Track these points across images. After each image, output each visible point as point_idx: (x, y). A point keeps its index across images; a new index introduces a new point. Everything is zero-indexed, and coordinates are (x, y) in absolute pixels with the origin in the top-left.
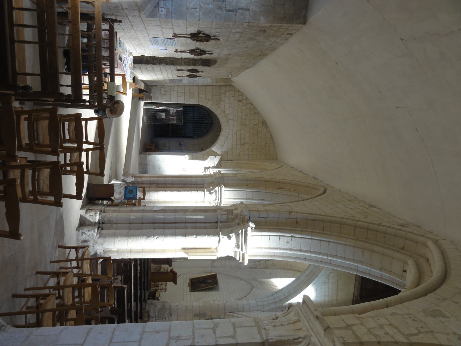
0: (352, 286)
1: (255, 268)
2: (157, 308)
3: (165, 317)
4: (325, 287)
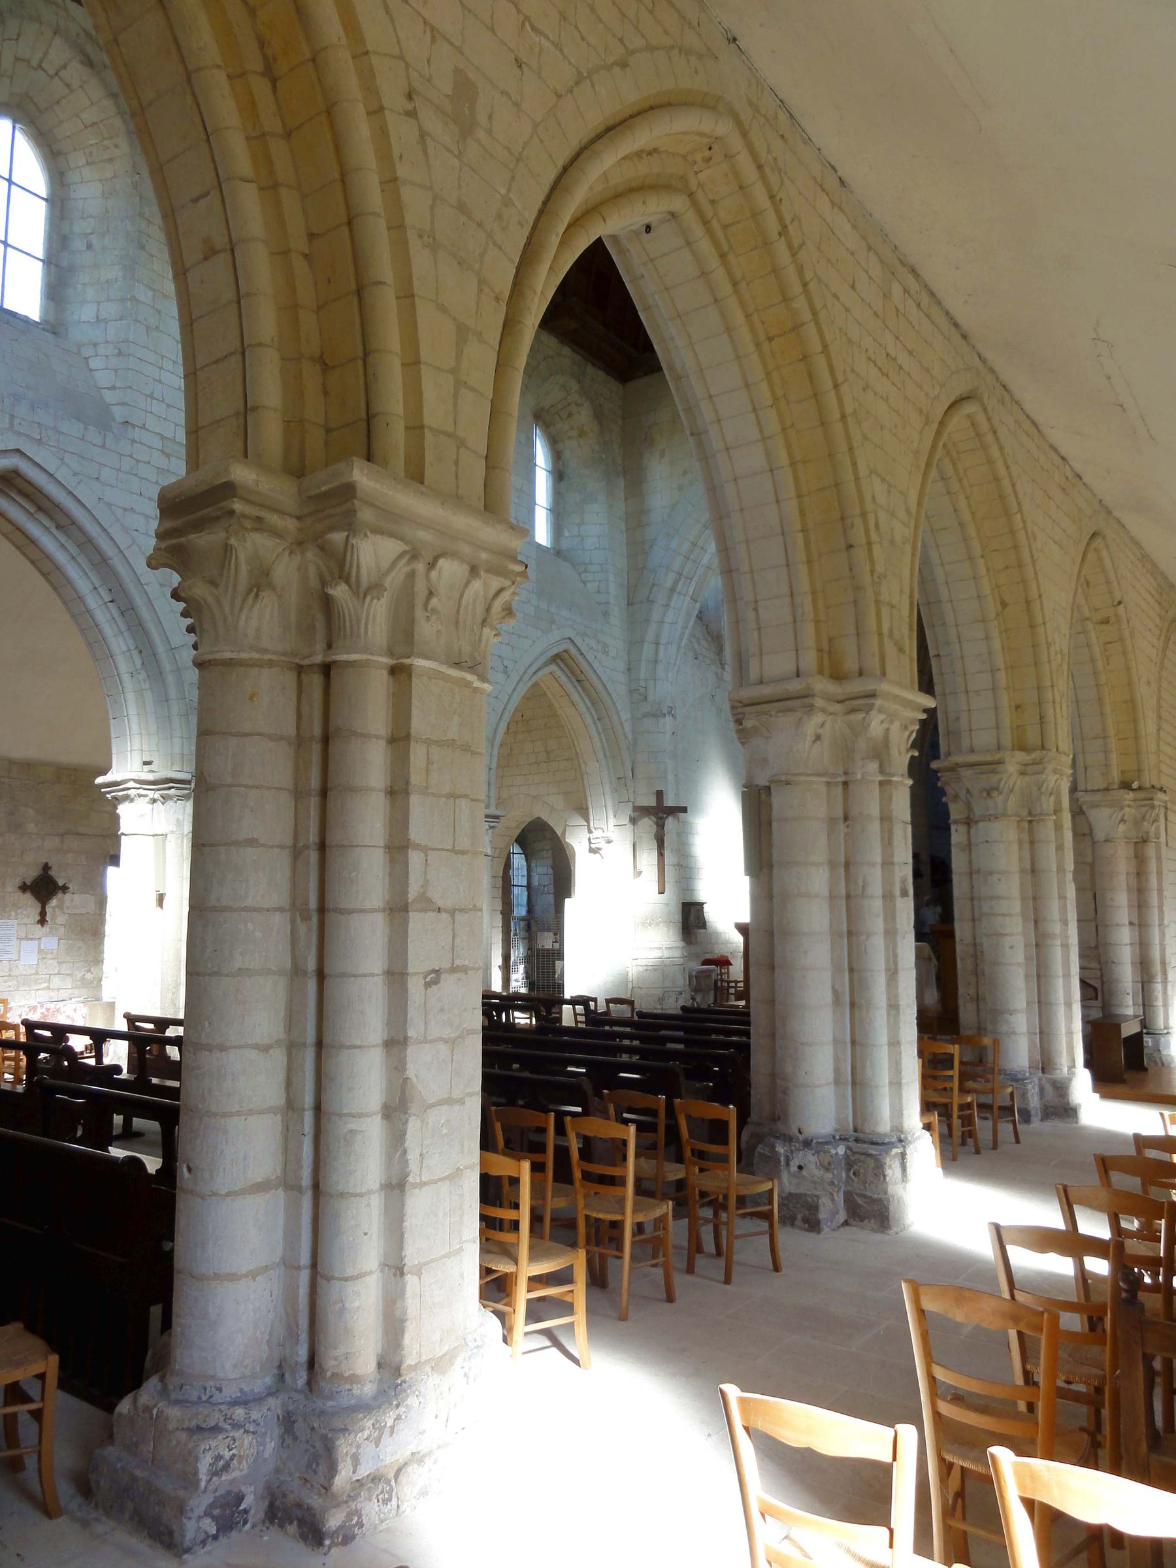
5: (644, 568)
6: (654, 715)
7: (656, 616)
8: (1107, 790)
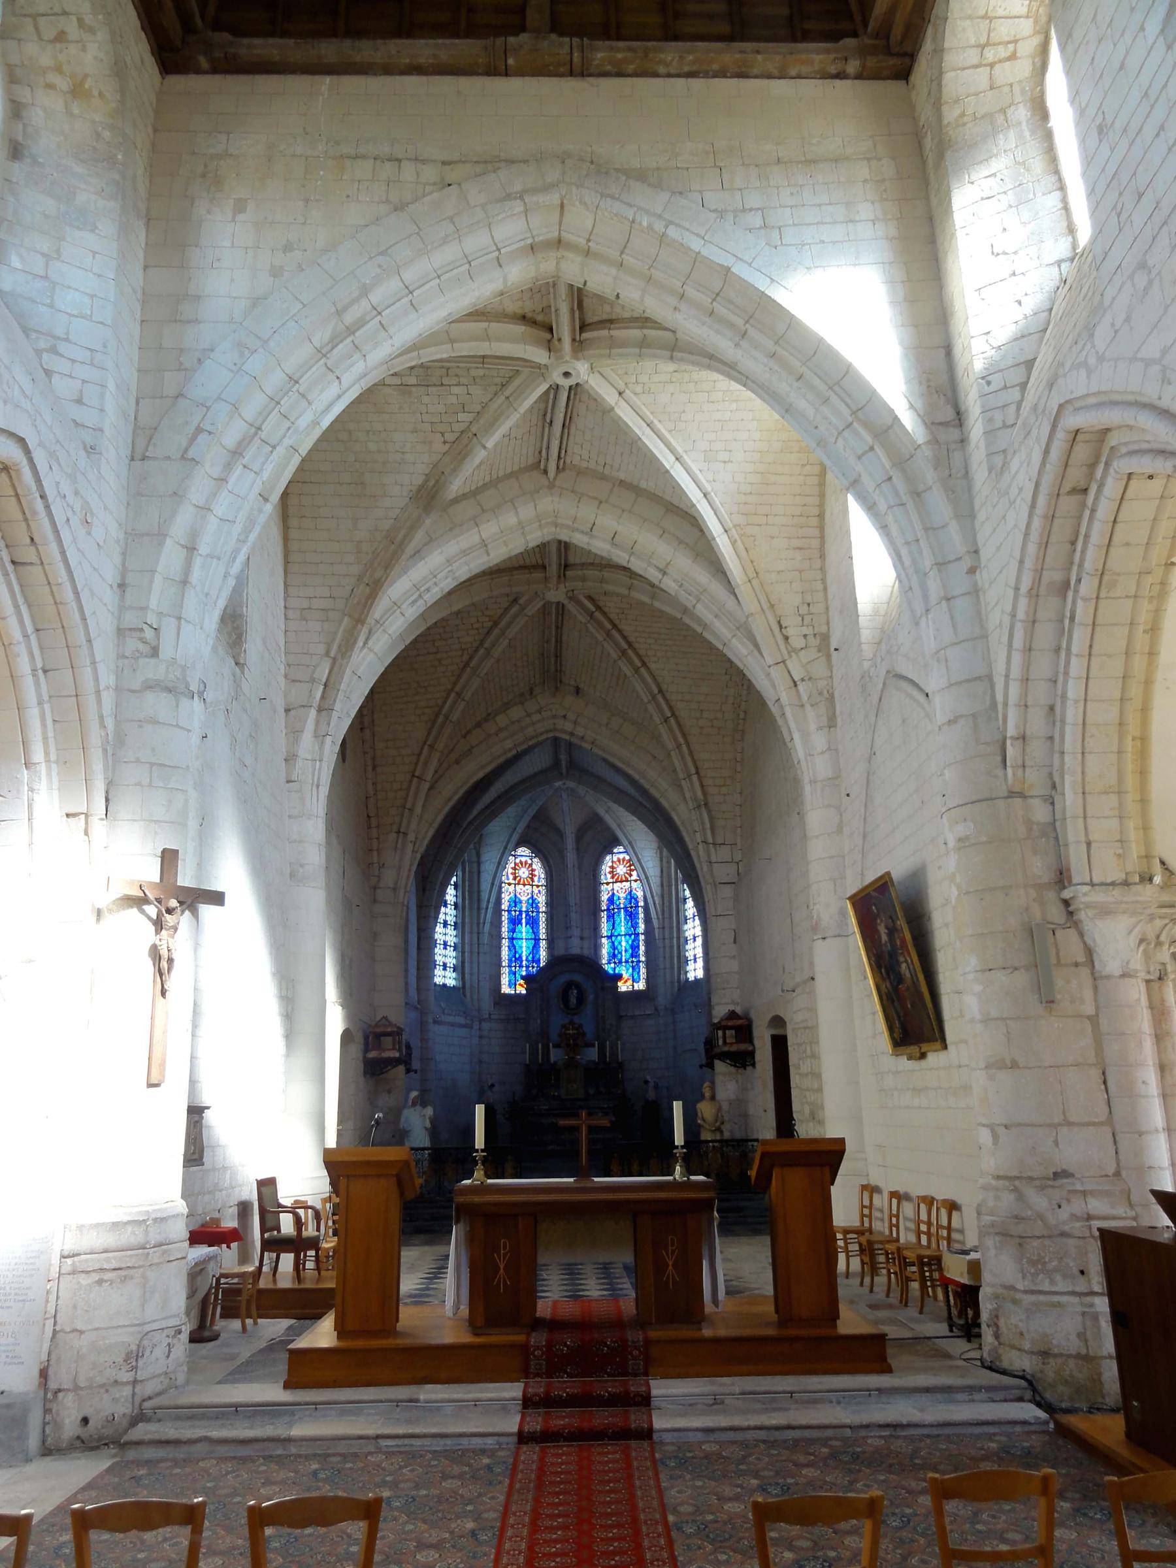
0: (779, 87)
1: (831, 699)
2: (1020, 1286)
3: (1078, 1224)
4: (794, 225)
5: (180, 395)
6: (169, 690)
7: (197, 492)
8: (1126, 883)
